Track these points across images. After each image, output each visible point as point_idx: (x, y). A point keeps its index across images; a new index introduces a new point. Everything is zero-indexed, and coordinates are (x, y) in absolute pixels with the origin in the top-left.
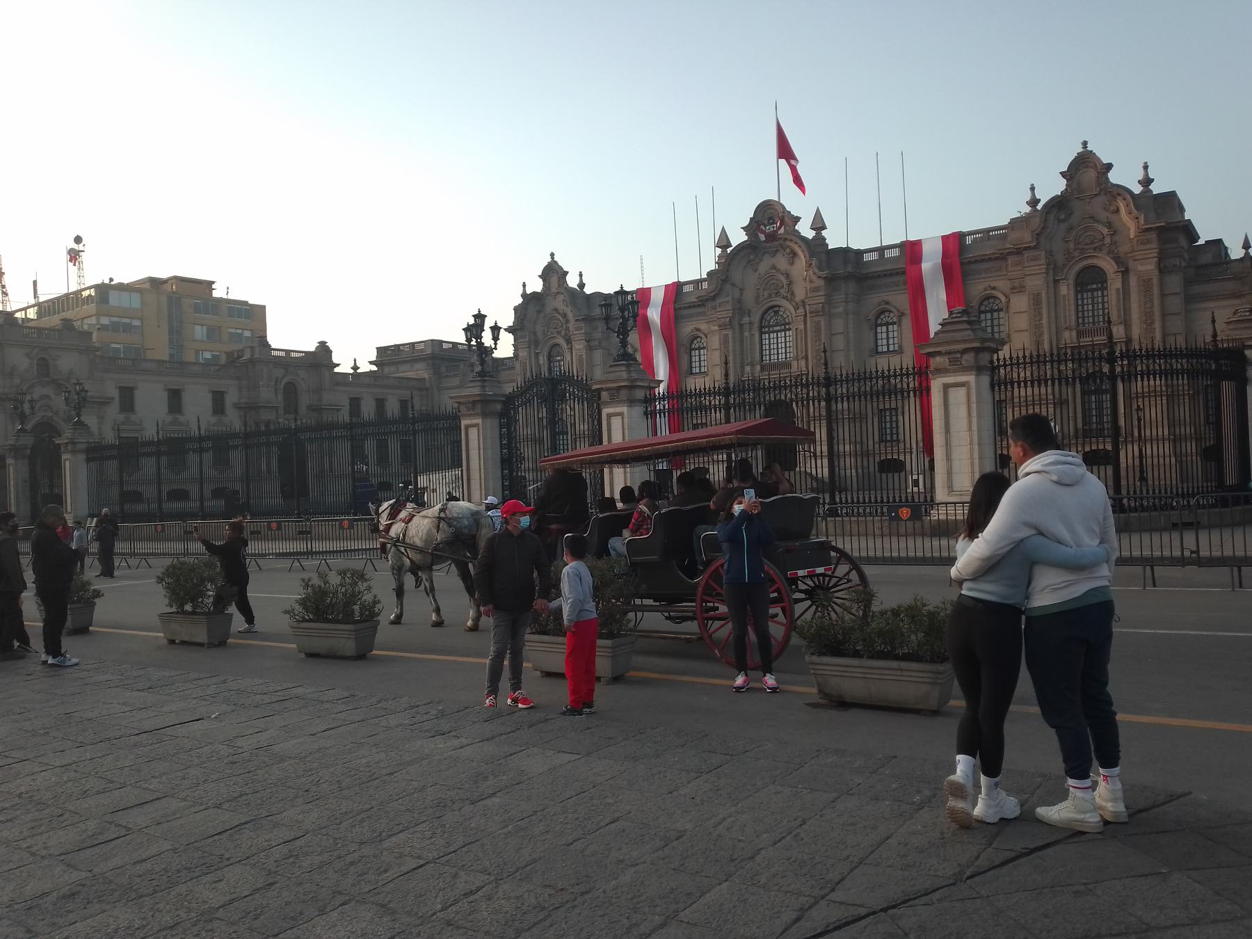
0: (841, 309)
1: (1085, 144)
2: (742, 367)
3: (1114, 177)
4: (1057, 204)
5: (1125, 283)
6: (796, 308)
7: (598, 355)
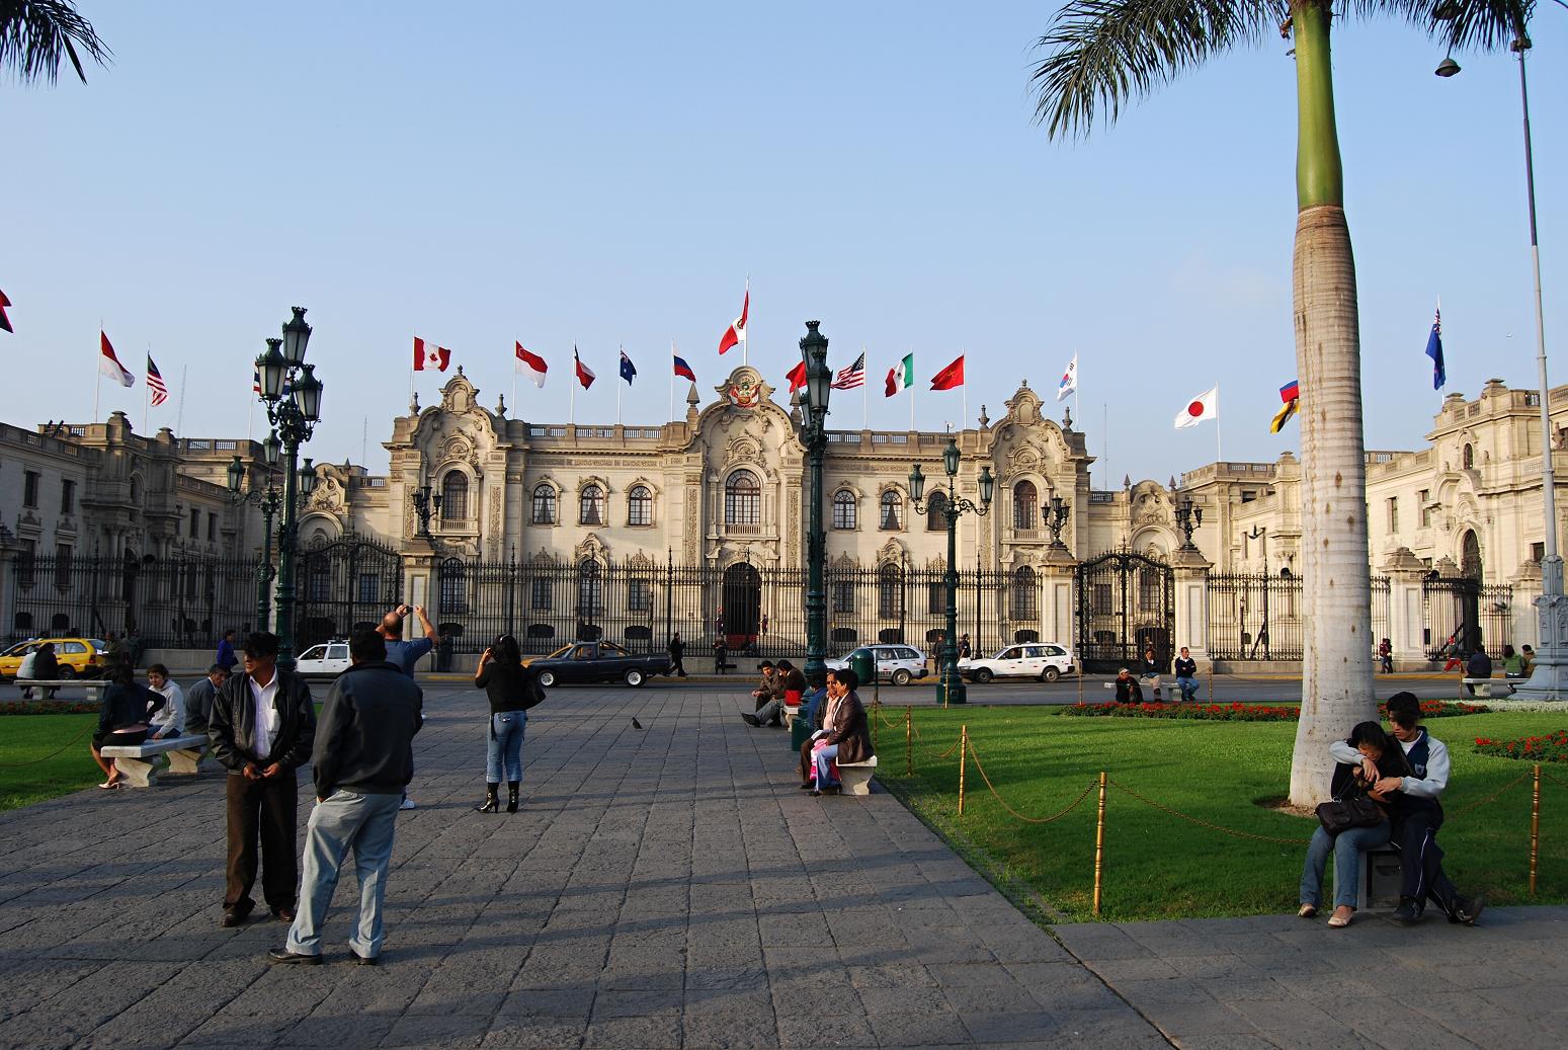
1: (1025, 382)
6: (769, 476)
7: (518, 489)
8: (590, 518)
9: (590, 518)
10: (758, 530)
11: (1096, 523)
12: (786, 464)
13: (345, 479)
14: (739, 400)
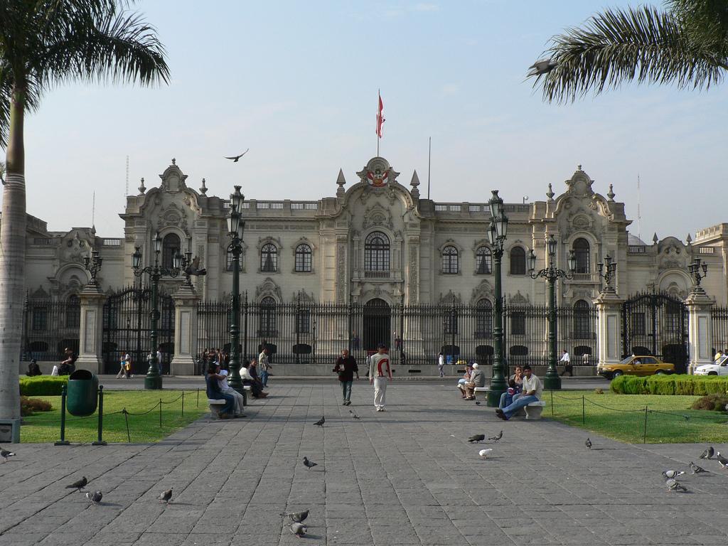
0: (428, 241)
2: (352, 272)
3: (595, 188)
4: (566, 199)
5: (600, 250)
7: (216, 246)
8: (268, 267)
9: (268, 267)
10: (388, 275)
11: (632, 268)
12: (408, 227)
13: (92, 241)
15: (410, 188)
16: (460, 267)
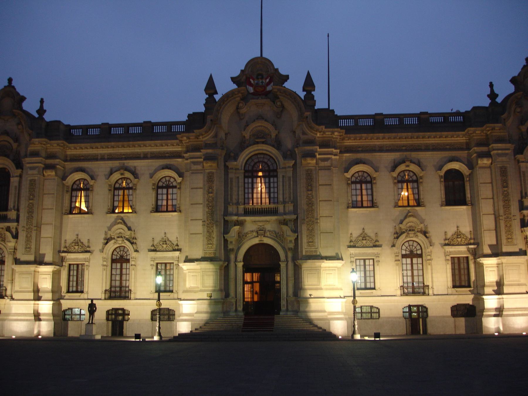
6: (285, 157)
14: (254, 89)
15: (302, 95)
16: (374, 198)
